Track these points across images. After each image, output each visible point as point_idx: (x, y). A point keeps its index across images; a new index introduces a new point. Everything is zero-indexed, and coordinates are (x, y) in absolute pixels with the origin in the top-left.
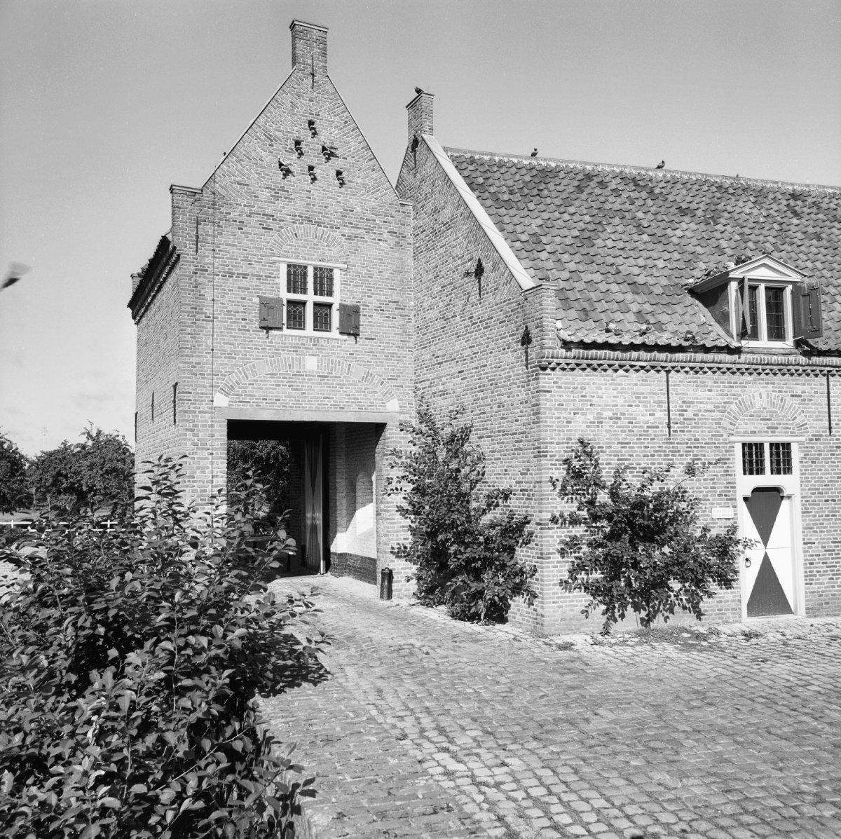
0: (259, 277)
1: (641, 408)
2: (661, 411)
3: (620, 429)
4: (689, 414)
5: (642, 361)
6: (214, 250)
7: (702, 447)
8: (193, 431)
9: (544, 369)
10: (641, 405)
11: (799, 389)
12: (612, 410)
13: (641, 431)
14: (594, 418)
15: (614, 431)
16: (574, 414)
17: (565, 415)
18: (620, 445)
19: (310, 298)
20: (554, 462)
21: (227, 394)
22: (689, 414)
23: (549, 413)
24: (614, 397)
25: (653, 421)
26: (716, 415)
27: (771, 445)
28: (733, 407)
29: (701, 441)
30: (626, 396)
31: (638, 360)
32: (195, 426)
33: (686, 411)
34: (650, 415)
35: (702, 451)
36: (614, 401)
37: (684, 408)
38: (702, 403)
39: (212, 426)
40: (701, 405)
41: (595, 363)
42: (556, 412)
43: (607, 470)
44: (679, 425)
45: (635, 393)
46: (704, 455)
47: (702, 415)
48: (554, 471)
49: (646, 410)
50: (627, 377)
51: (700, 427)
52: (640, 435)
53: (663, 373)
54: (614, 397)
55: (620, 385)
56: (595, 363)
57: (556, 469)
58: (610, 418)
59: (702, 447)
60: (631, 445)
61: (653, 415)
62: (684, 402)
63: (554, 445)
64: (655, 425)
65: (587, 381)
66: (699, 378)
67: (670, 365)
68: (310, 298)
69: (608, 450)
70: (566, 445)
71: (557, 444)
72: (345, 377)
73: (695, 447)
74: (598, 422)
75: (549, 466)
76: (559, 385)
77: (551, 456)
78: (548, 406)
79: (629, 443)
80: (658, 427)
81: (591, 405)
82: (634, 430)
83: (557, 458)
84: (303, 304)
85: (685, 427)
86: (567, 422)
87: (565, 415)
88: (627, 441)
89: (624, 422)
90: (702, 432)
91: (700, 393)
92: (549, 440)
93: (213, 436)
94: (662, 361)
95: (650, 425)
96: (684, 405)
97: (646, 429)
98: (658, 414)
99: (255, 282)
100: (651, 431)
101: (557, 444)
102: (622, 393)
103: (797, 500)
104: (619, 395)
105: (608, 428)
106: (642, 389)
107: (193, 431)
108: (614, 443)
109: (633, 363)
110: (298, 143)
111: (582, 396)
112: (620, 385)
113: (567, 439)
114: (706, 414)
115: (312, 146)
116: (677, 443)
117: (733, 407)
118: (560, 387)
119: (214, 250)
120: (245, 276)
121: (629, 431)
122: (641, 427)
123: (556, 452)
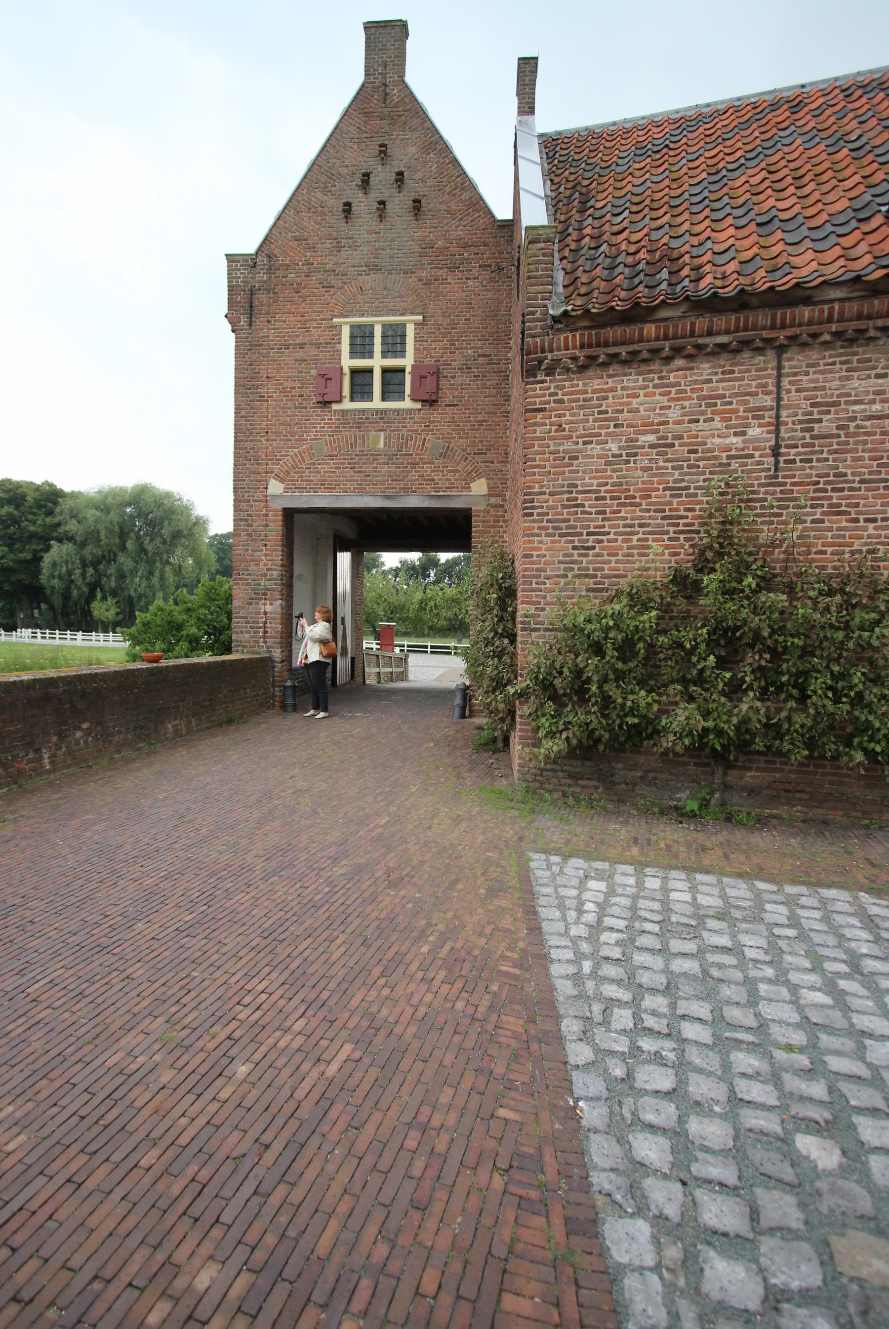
0: (318, 345)
1: (717, 423)
2: (760, 426)
3: (669, 465)
4: (827, 425)
5: (719, 333)
6: (269, 321)
7: (851, 489)
8: (246, 520)
10: (717, 418)
12: (657, 431)
13: (714, 465)
14: (620, 448)
15: (658, 468)
16: (584, 443)
17: (568, 445)
18: (668, 493)
20: (544, 524)
21: (282, 481)
22: (827, 425)
23: (540, 446)
24: (662, 408)
25: (740, 445)
29: (850, 477)
30: (686, 403)
31: (710, 333)
32: (249, 515)
33: (820, 421)
34: (735, 434)
35: (851, 497)
36: (660, 415)
37: (816, 416)
38: (860, 402)
39: (267, 515)
40: (856, 408)
41: (623, 351)
42: (551, 443)
43: (641, 536)
44: (800, 449)
45: (705, 398)
46: (857, 505)
47: (858, 427)
48: (543, 538)
49: (727, 427)
50: (691, 369)
51: (850, 451)
52: (711, 473)
53: (771, 354)
54: (662, 408)
55: (673, 385)
56: (623, 351)
57: (547, 535)
58: (651, 446)
59: (851, 489)
60: (692, 491)
61: (744, 434)
62: (813, 405)
63: (546, 497)
64: (746, 452)
65: (610, 384)
66: (855, 354)
67: (781, 336)
68: (377, 362)
69: (644, 502)
70: (566, 496)
71: (552, 494)
72: (418, 455)
73: (833, 490)
74: (628, 455)
75: (536, 531)
76: (560, 397)
77: (539, 514)
78: (538, 434)
79: (688, 488)
80: (752, 456)
81: (615, 426)
82: (701, 464)
83: (550, 517)
84: (370, 371)
85: (812, 453)
86: (570, 458)
87: (568, 445)
88: (684, 484)
89: (680, 450)
90: (854, 459)
91: (855, 383)
92: (536, 490)
93: (267, 526)
94: (764, 328)
95: (733, 452)
96: (815, 410)
97: (724, 461)
98: (754, 432)
99: (312, 351)
100: (734, 464)
101: (552, 494)
102: (678, 399)
104: (672, 404)
105: (646, 463)
106: (720, 388)
107: (246, 520)
108: (657, 490)
109: (700, 341)
110: (367, 175)
111: (600, 413)
112: (673, 385)
113: (569, 486)
114: (868, 423)
115: (382, 177)
116: (793, 484)
118: (561, 401)
119: (269, 321)
120: (302, 346)
121: (689, 467)
122: (715, 458)
123: (548, 508)
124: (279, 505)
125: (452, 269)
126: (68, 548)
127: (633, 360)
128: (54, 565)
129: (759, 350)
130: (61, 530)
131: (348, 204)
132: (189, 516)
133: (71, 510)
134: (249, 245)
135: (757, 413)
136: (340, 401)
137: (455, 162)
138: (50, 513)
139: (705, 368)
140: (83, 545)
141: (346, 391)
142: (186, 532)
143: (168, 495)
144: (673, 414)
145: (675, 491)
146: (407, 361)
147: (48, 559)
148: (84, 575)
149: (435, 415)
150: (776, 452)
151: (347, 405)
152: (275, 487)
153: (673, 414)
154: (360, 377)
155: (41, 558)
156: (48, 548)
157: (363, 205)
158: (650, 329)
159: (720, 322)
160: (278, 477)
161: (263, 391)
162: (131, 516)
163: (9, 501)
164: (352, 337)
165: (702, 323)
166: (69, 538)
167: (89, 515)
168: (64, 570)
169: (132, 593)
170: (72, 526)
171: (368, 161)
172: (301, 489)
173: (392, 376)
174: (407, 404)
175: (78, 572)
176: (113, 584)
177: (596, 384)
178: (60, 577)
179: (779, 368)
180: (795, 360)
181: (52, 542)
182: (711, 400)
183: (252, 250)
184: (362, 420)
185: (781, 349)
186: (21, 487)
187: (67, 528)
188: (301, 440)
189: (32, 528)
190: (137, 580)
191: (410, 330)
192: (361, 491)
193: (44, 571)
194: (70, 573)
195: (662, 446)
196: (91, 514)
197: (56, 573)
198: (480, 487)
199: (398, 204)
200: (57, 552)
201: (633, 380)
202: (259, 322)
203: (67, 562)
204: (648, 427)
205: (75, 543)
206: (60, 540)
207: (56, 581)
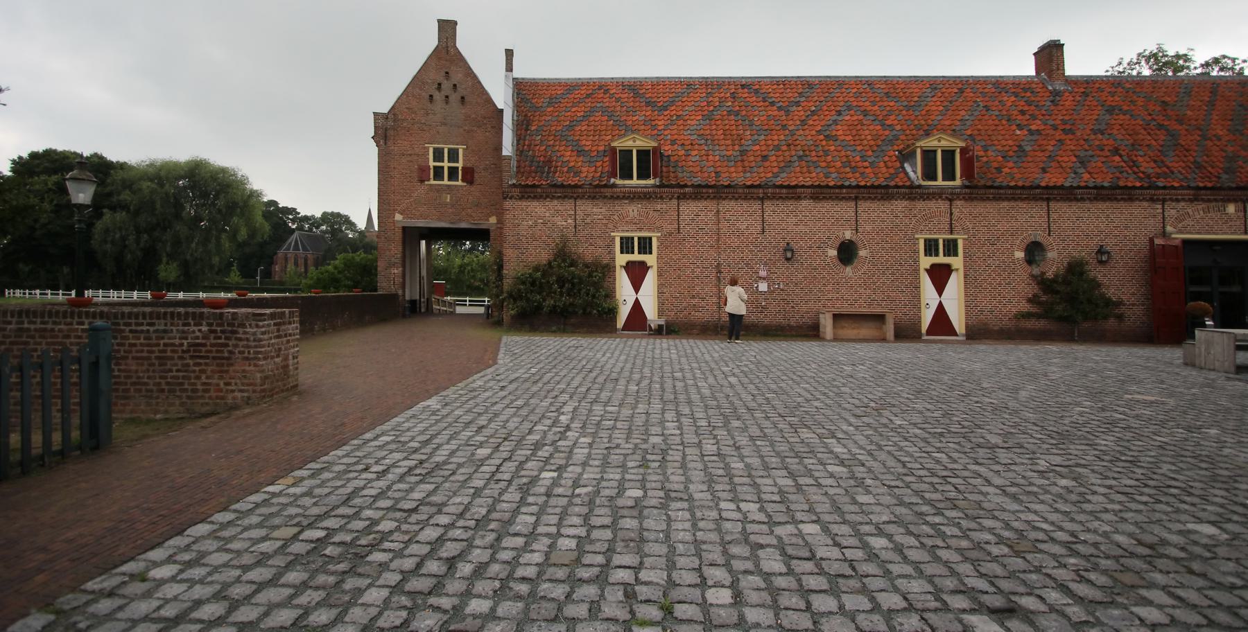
0: (418, 155)
4: (588, 221)
9: (505, 198)
11: (659, 207)
19: (446, 164)
26: (604, 221)
27: (639, 238)
28: (615, 217)
68: (446, 164)
89: (549, 225)
99: (416, 158)
103: (655, 268)
110: (440, 84)
115: (446, 86)
117: (615, 217)
120: (410, 155)
124: (400, 225)
125: (479, 127)
126: (121, 216)
127: (535, 198)
128: (107, 231)
129: (570, 198)
130: (115, 199)
131: (431, 96)
132: (245, 189)
133: (123, 181)
134: (385, 108)
136: (429, 180)
137: (479, 82)
139: (556, 202)
140: (137, 213)
142: (241, 204)
143: (224, 170)
144: (547, 214)
145: (548, 237)
146: (460, 165)
147: (99, 225)
148: (138, 241)
149: (472, 189)
150: (575, 227)
151: (432, 182)
152: (398, 217)
153: (547, 214)
154: (438, 173)
157: (438, 97)
158: (539, 190)
159: (558, 190)
160: (399, 213)
161: (392, 173)
162: (185, 187)
164: (434, 153)
165: (553, 190)
166: (124, 207)
167: (144, 187)
168: (118, 236)
169: (188, 257)
170: (126, 196)
171: (440, 78)
172: (411, 218)
173: (453, 173)
174: (460, 183)
176: (168, 249)
177: (524, 203)
180: (579, 202)
181: (105, 210)
183: (386, 111)
184: (439, 189)
185: (575, 199)
186: (68, 158)
187: (122, 197)
188: (410, 196)
190: (193, 245)
191: (461, 152)
192: (439, 220)
193: (96, 236)
194: (124, 239)
196: (145, 185)
197: (109, 239)
198: (493, 220)
199: (454, 98)
201: (535, 203)
202: (390, 143)
203: (120, 229)
205: (128, 211)
206: (113, 208)
207: (109, 246)
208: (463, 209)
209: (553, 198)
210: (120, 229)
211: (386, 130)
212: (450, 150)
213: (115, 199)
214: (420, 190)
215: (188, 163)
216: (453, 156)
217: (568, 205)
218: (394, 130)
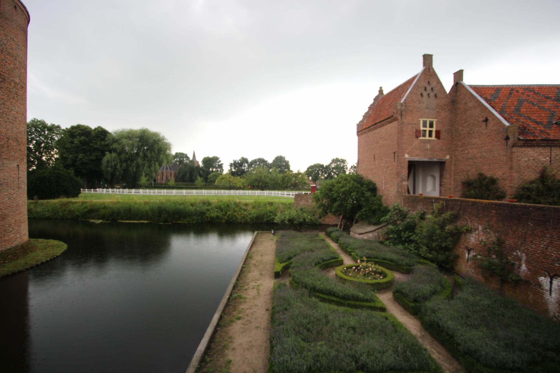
17: (519, 159)
19: (428, 129)
68: (428, 129)
115: (429, 88)
120: (412, 124)
124: (407, 160)
126: (114, 155)
128: (108, 162)
135: (548, 155)
138: (103, 140)
139: (540, 148)
141: (422, 135)
146: (434, 129)
147: (105, 159)
148: (121, 166)
150: (550, 161)
152: (407, 156)
153: (536, 155)
155: (101, 159)
156: (104, 155)
157: (425, 94)
158: (534, 142)
160: (407, 153)
163: (83, 134)
166: (115, 150)
171: (426, 85)
172: (412, 156)
175: (119, 165)
178: (111, 167)
179: (551, 149)
180: (553, 149)
182: (541, 153)
184: (425, 142)
188: (412, 145)
189: (96, 146)
190: (145, 168)
194: (116, 165)
195: (534, 160)
197: (110, 165)
198: (448, 157)
199: (432, 94)
200: (108, 156)
201: (529, 149)
204: (531, 156)
205: (117, 153)
206: (110, 152)
207: (109, 168)
208: (435, 152)
209: (541, 146)
210: (114, 161)
211: (402, 111)
212: (430, 121)
213: (111, 147)
214: (416, 142)
215: (140, 130)
216: (431, 125)
217: (546, 151)
218: (405, 111)
